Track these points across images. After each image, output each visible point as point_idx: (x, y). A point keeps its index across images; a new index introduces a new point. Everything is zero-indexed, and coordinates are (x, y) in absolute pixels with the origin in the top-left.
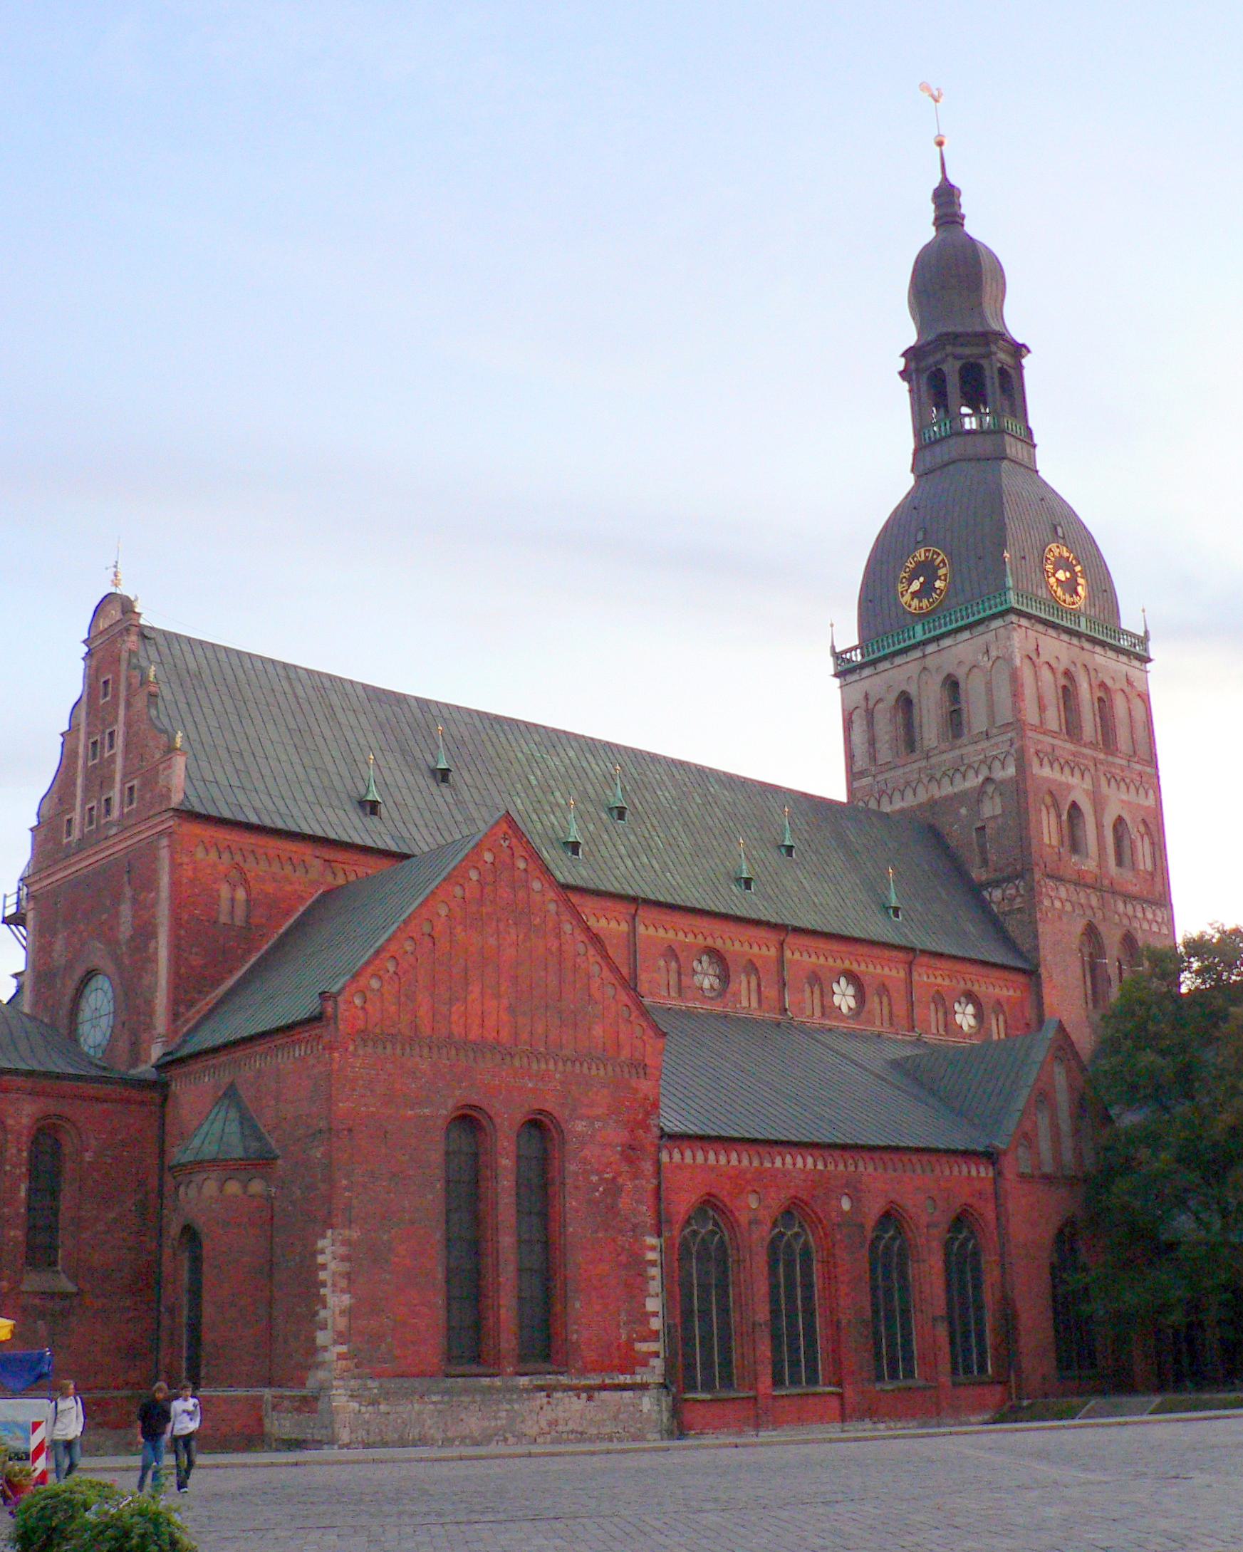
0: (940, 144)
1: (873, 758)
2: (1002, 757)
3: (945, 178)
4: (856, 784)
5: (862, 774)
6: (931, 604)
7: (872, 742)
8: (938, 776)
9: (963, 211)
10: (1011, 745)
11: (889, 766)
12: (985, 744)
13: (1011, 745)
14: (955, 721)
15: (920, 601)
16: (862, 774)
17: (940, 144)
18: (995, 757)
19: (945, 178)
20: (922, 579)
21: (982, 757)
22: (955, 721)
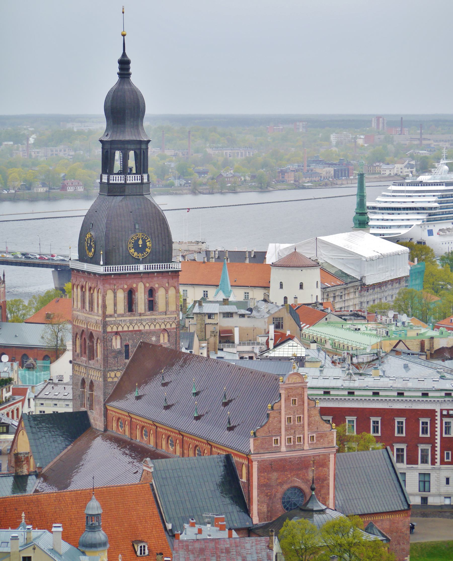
0: (124, 35)
1: (115, 311)
2: (171, 323)
3: (124, 54)
4: (107, 319)
5: (111, 316)
6: (144, 256)
7: (115, 305)
8: (144, 324)
9: (118, 65)
10: (175, 319)
11: (122, 316)
12: (164, 316)
13: (175, 319)
14: (151, 305)
15: (135, 252)
16: (111, 316)
17: (124, 35)
18: (168, 322)
19: (124, 54)
20: (140, 246)
21: (162, 321)
22: (151, 305)
